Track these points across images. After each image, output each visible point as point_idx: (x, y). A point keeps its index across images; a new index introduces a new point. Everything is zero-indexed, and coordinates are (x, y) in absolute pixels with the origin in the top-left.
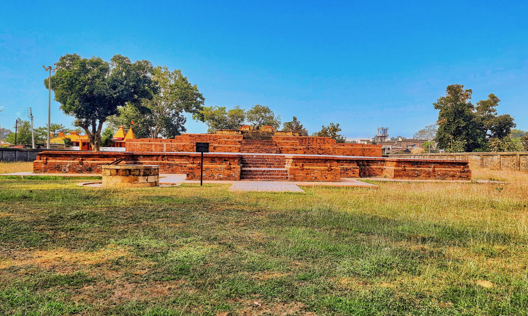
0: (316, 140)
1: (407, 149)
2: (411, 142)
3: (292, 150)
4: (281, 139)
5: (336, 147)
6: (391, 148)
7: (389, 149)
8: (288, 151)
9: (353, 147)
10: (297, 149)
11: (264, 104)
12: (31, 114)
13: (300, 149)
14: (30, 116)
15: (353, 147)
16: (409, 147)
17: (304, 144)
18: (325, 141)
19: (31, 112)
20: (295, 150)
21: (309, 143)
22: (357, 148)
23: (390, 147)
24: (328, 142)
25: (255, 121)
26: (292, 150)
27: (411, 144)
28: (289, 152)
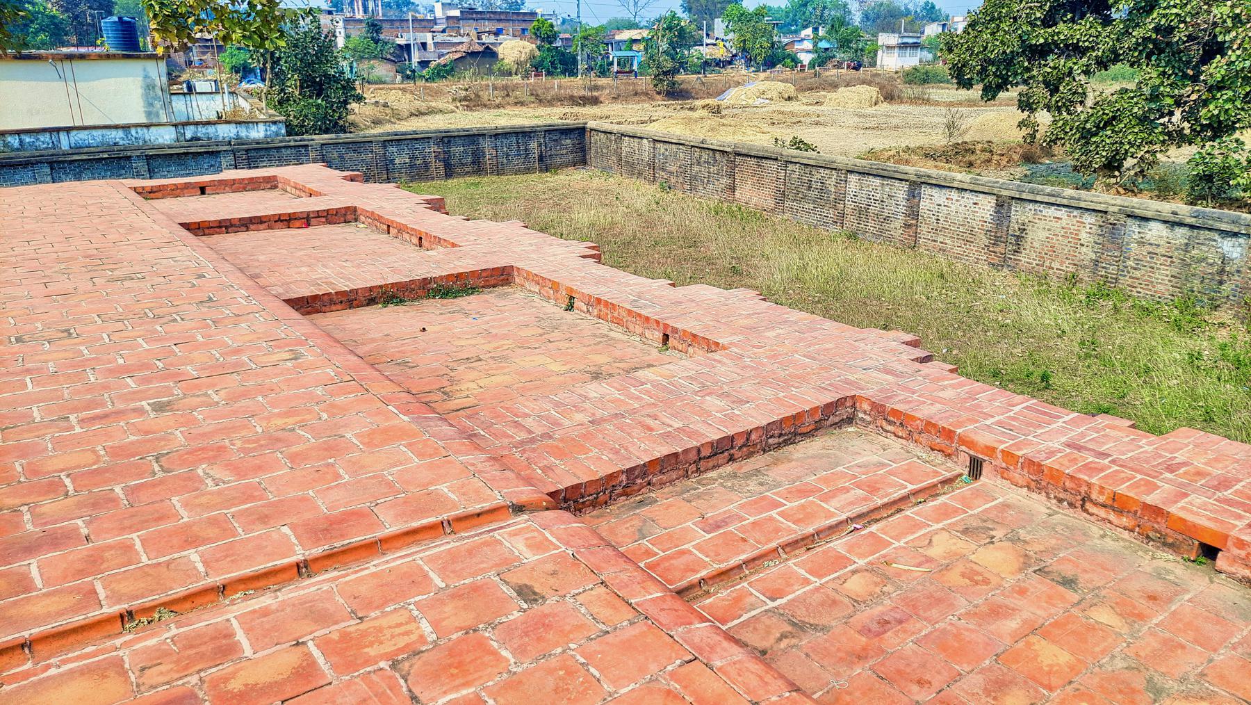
1: (488, 47)
2: (488, 19)
6: (430, 42)
7: (424, 45)
16: (486, 39)
23: (428, 38)
27: (489, 26)
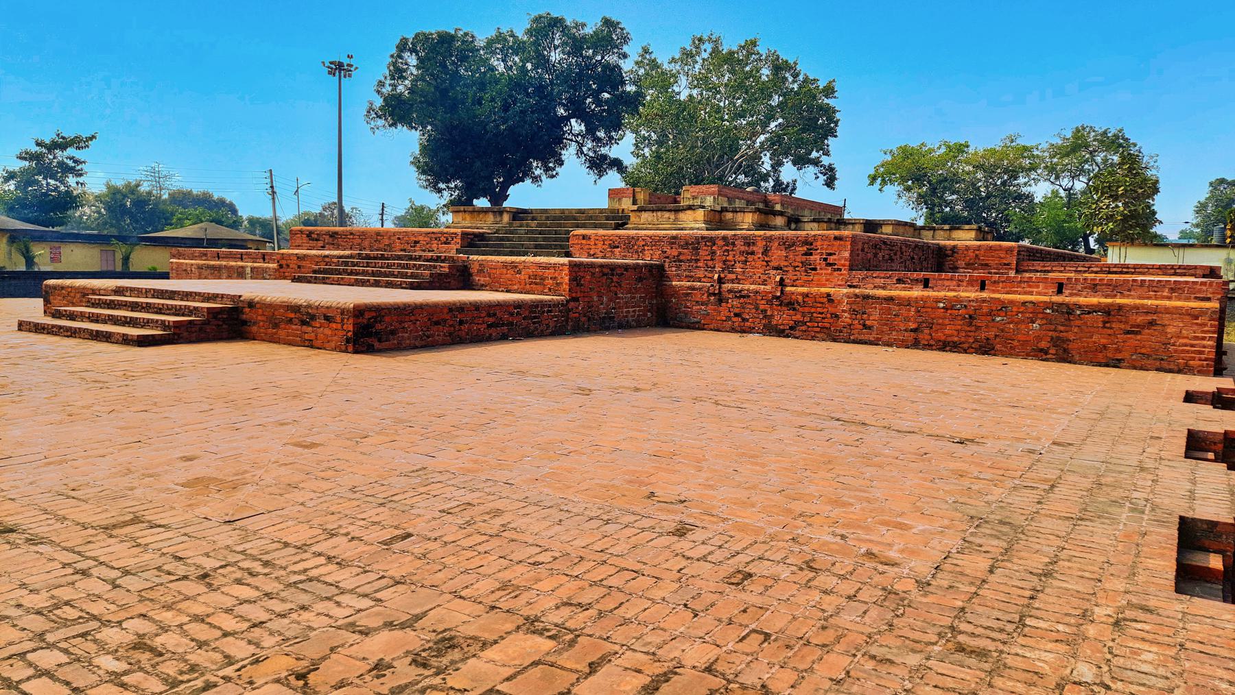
0: (765, 252)
3: (290, 321)
4: (600, 244)
5: (871, 292)
8: (276, 326)
9: (984, 295)
10: (313, 317)
11: (1102, 121)
12: (272, 187)
13: (327, 318)
14: (270, 191)
15: (984, 295)
17: (700, 274)
18: (816, 258)
19: (272, 182)
20: (304, 323)
21: (728, 267)
22: (1012, 302)
24: (831, 259)
25: (1066, 180)
26: (290, 321)
28: (282, 333)
